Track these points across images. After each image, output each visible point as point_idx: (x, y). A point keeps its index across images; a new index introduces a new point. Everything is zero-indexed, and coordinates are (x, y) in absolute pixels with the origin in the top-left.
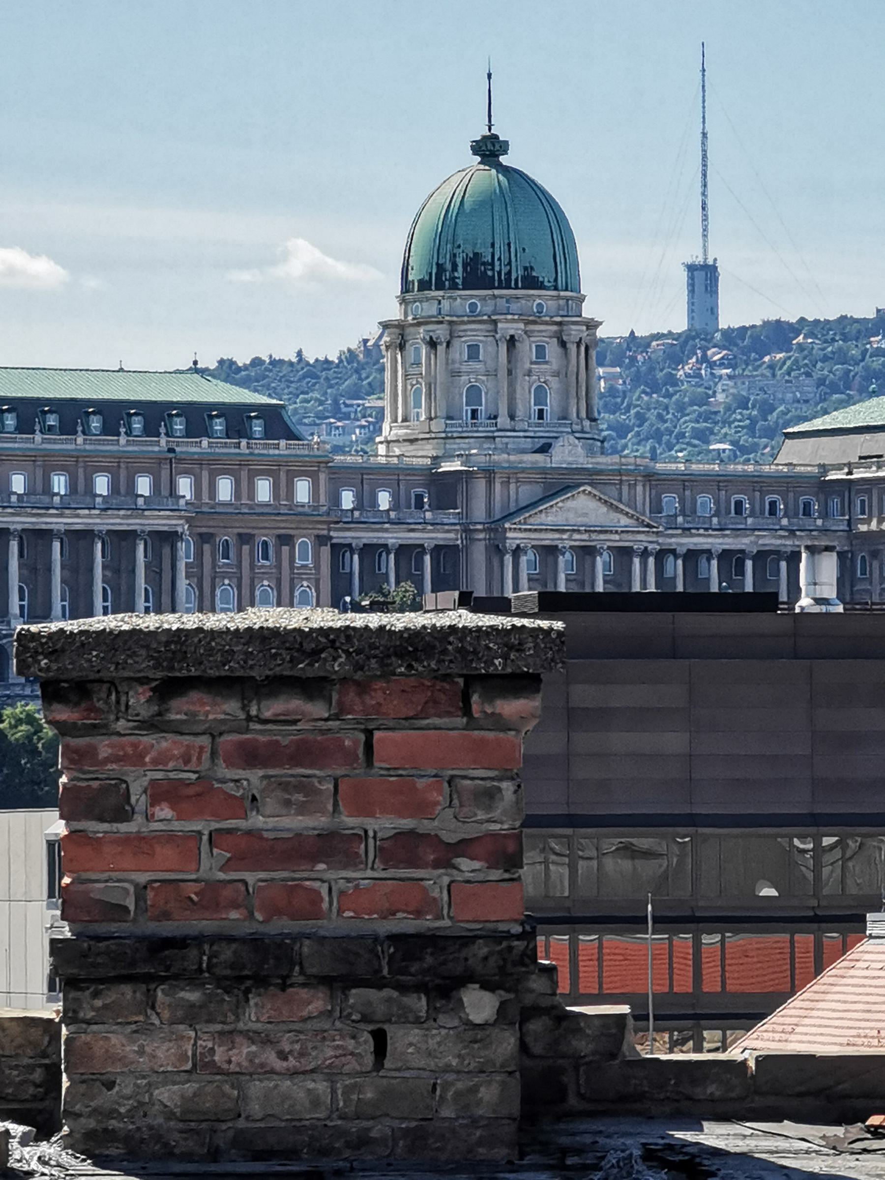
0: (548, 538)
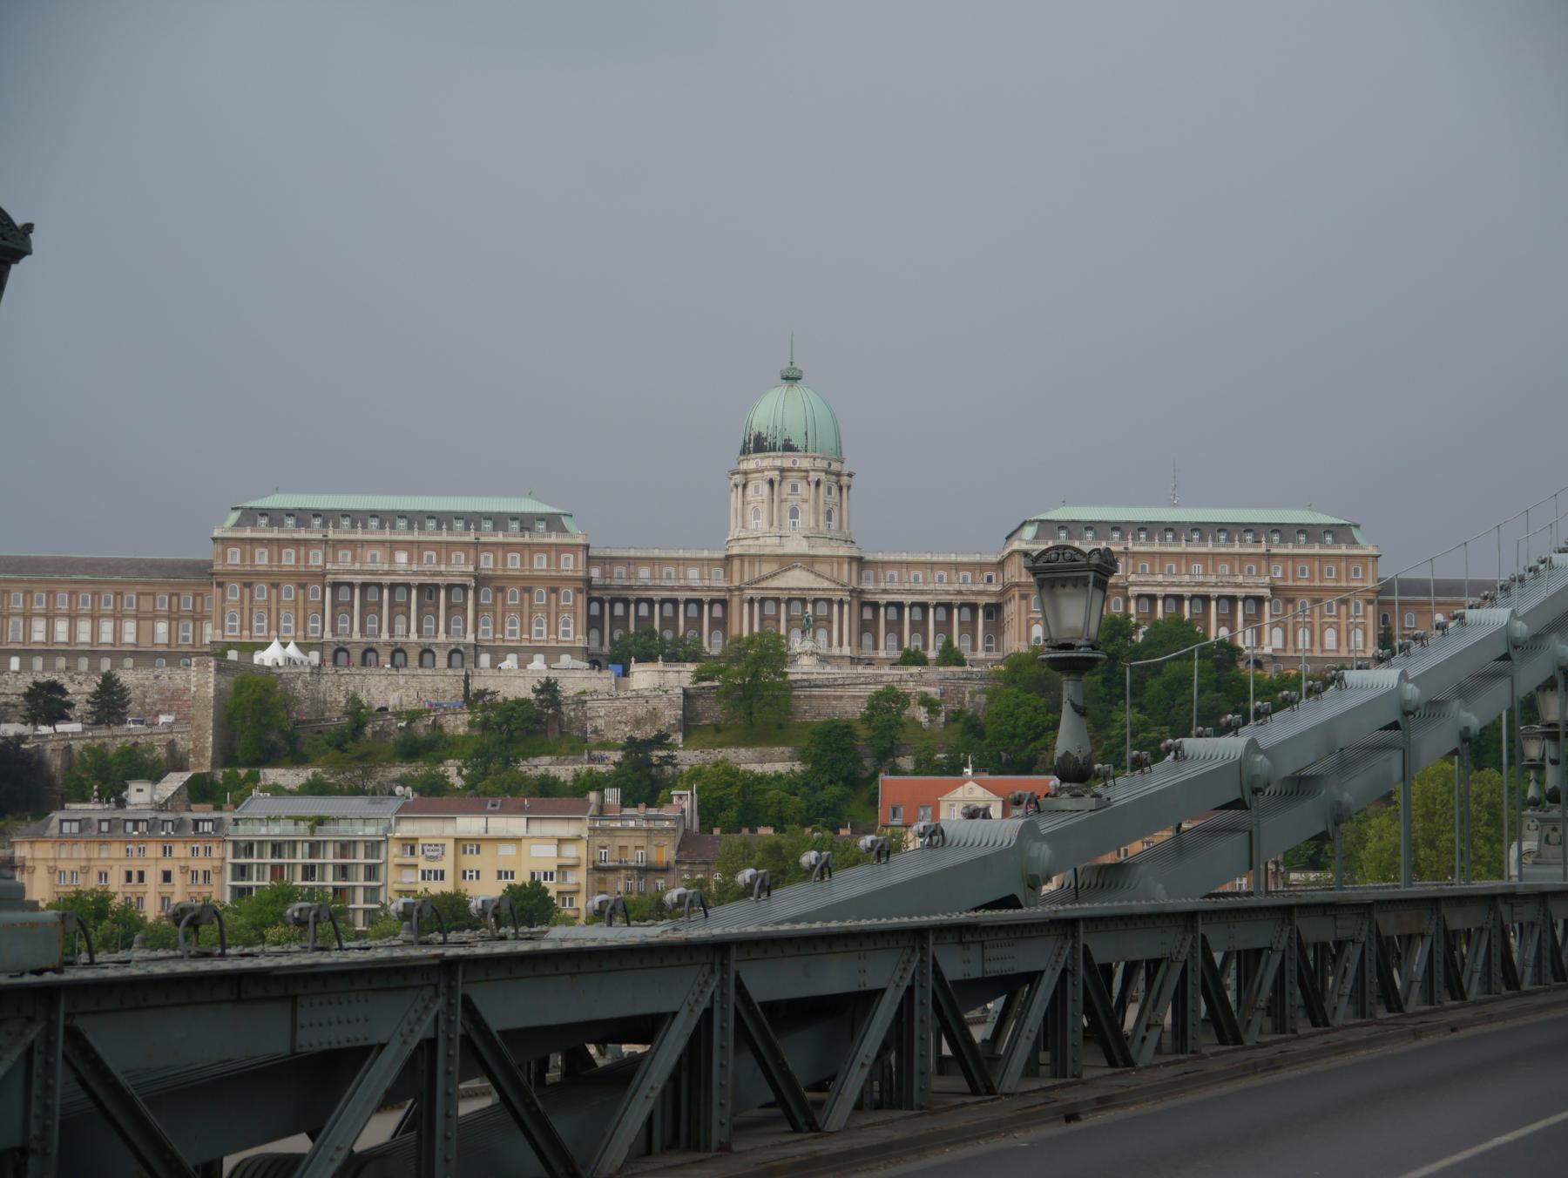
0: (773, 594)
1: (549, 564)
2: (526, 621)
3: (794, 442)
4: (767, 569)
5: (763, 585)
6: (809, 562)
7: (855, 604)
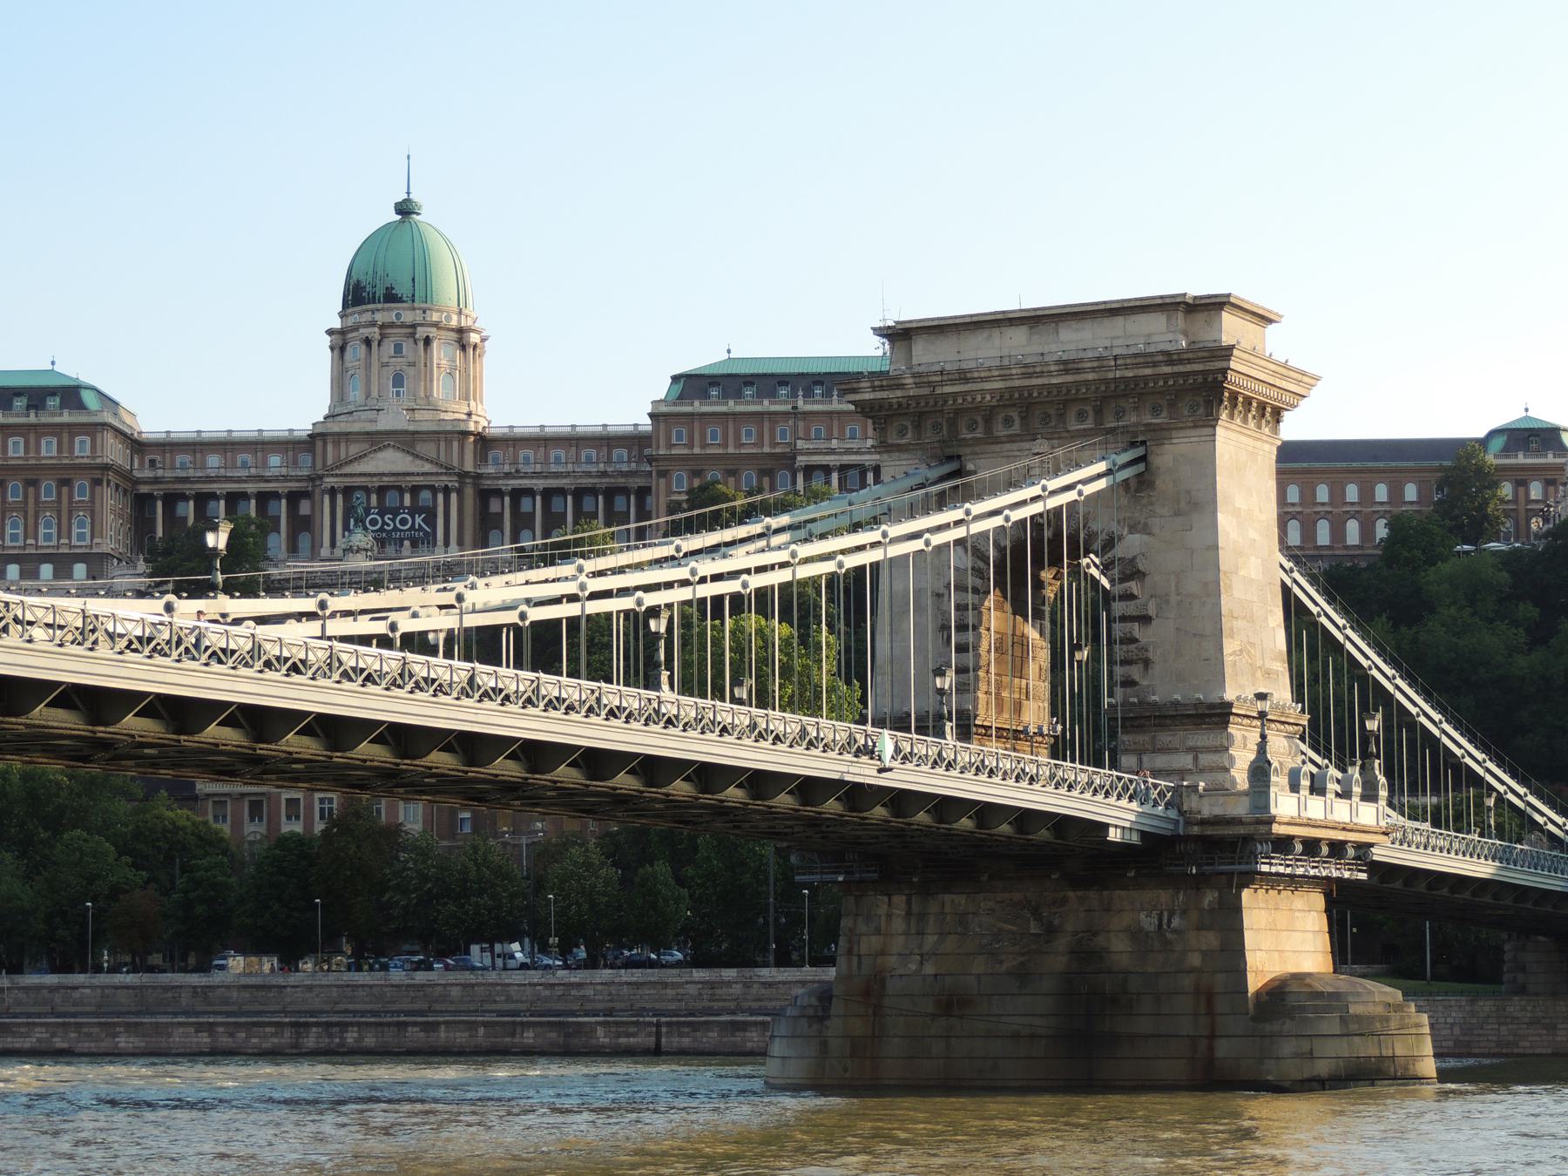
0: (358, 481)
1: (60, 450)
2: (31, 521)
3: (398, 291)
4: (354, 449)
5: (348, 470)
6: (407, 440)
7: (469, 492)
